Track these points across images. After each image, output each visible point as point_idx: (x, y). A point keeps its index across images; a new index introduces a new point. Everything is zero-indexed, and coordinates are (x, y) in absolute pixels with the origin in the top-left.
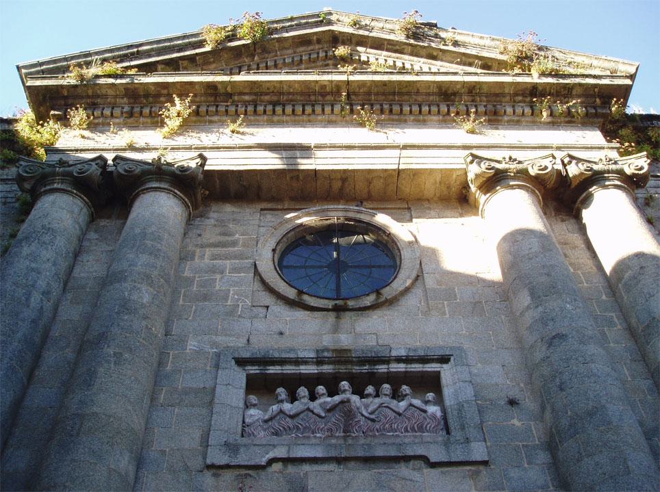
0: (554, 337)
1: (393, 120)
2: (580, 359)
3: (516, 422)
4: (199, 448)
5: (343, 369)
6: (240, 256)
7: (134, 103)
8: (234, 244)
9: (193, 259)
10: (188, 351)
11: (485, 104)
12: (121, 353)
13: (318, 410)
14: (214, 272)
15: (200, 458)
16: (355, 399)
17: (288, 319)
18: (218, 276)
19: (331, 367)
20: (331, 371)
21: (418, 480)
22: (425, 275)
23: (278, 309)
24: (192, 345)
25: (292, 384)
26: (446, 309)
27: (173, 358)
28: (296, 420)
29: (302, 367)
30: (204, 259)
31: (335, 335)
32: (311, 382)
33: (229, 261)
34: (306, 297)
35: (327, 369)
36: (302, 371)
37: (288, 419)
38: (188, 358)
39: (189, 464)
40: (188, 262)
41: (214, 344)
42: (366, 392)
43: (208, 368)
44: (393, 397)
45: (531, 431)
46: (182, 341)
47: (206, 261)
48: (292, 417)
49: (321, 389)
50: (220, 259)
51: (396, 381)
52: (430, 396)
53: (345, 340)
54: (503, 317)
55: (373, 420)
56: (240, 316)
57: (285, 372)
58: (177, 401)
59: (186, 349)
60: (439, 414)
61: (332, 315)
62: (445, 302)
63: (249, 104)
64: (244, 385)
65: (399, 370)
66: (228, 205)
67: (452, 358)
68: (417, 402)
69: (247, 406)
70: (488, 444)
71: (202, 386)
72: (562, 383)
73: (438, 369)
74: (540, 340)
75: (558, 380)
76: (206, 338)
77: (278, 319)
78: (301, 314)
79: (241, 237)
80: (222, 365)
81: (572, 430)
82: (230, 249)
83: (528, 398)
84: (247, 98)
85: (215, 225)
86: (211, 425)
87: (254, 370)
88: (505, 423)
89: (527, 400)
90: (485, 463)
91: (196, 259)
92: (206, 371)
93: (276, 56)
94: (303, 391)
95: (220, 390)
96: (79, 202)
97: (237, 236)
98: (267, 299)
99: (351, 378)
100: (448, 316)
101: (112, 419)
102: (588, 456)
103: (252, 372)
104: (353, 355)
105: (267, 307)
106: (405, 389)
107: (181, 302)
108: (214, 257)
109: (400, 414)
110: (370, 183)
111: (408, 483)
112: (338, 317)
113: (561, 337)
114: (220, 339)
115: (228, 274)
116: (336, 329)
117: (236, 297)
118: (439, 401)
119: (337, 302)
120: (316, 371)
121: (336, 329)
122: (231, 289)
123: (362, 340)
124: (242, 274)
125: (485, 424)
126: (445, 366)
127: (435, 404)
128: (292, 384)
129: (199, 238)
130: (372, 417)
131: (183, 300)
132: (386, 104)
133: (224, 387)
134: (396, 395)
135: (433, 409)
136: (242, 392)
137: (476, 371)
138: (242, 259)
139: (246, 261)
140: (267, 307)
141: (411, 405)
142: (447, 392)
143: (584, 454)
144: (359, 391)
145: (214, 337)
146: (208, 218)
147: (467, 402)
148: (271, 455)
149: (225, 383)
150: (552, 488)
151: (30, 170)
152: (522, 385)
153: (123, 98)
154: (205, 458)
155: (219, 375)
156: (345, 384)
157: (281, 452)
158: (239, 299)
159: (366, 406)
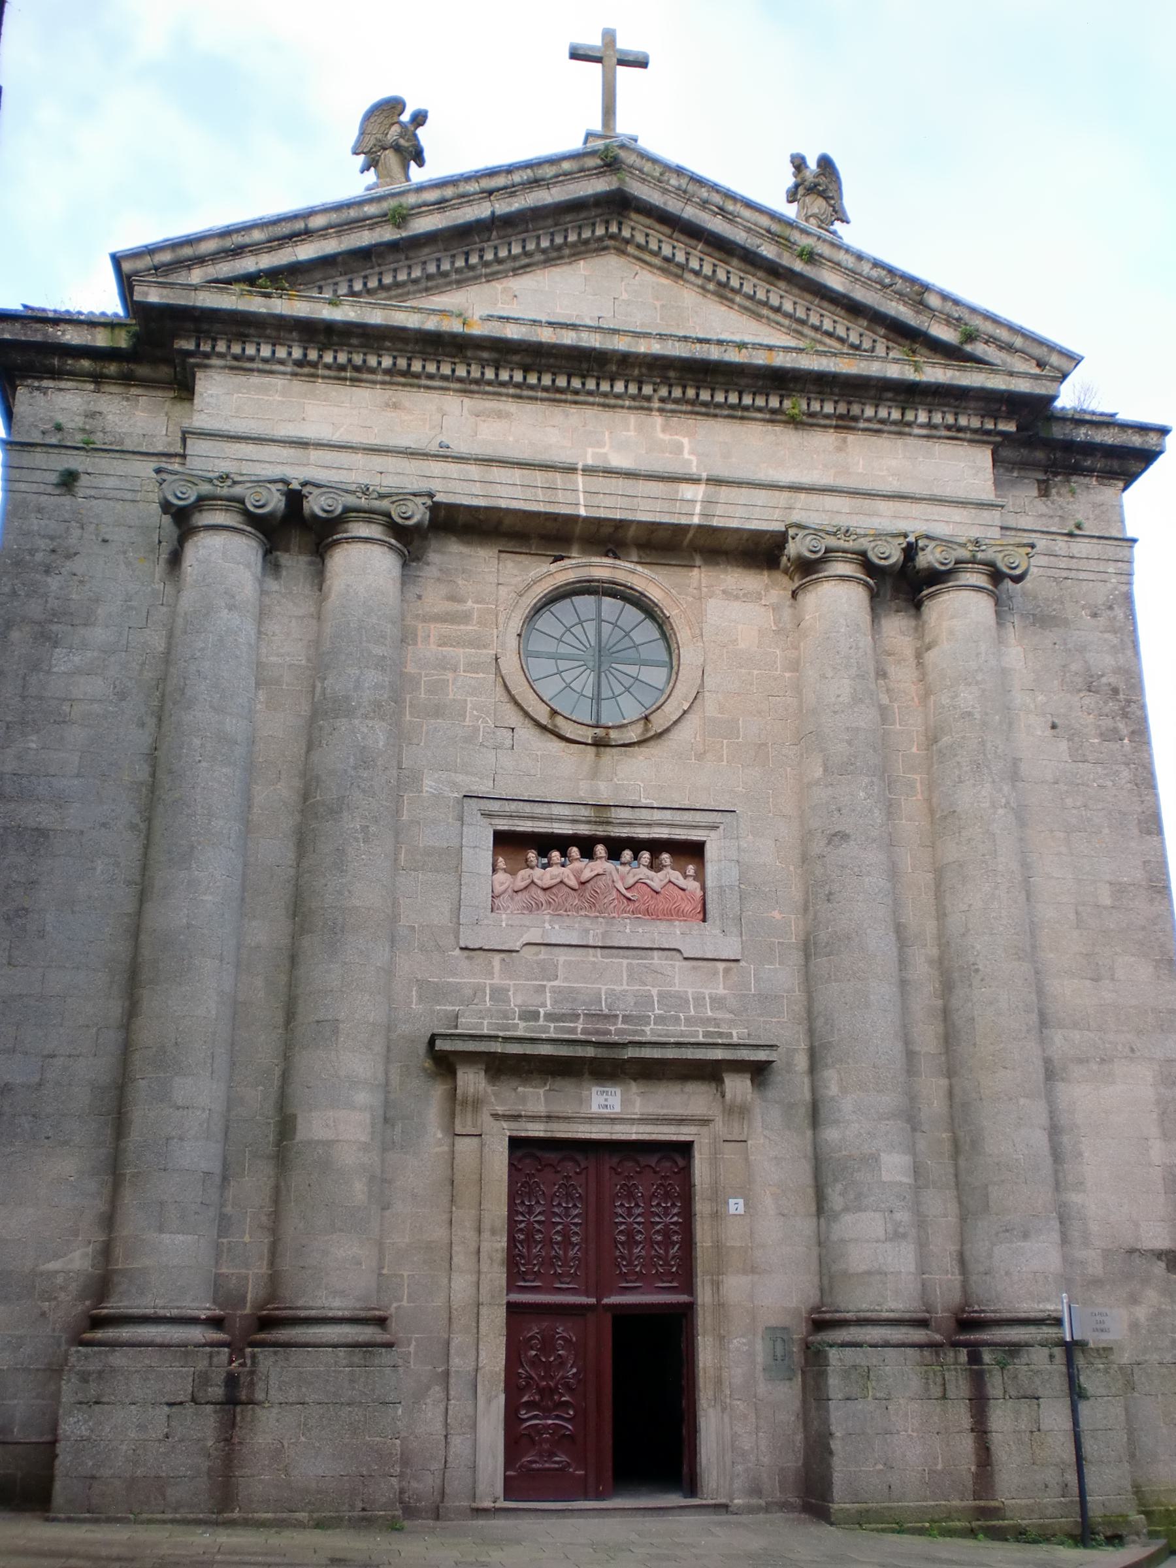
0: (835, 835)
1: (697, 413)
2: (856, 869)
3: (776, 914)
4: (450, 924)
5: (600, 831)
6: (476, 643)
7: (310, 341)
8: (465, 618)
9: (415, 644)
10: (424, 794)
11: (836, 398)
12: (368, 827)
13: (573, 882)
14: (445, 669)
15: (452, 937)
16: (610, 866)
17: (539, 753)
18: (450, 676)
19: (587, 827)
20: (587, 833)
21: (670, 974)
22: (707, 694)
23: (527, 733)
24: (429, 784)
26: (725, 752)
27: (409, 804)
28: (548, 892)
29: (555, 825)
30: (429, 643)
31: (593, 782)
32: (561, 843)
33: (462, 650)
34: (560, 721)
35: (584, 830)
36: (556, 831)
37: (539, 891)
38: (426, 804)
39: (440, 943)
40: (409, 647)
41: (454, 785)
42: (623, 860)
43: (450, 820)
44: (651, 866)
45: (790, 926)
46: (416, 779)
47: (433, 647)
48: (545, 890)
49: (574, 851)
50: (451, 646)
51: (656, 847)
52: (691, 869)
53: (604, 793)
54: (789, 769)
55: (629, 899)
56: (482, 745)
57: (536, 830)
58: (420, 864)
59: (422, 792)
60: (699, 893)
61: (591, 750)
62: (725, 741)
63: (488, 365)
64: (491, 844)
65: (662, 836)
66: (454, 539)
67: (722, 827)
68: (676, 876)
69: (494, 870)
70: (744, 938)
71: (445, 845)
72: (830, 893)
73: (704, 839)
74: (820, 831)
75: (827, 887)
76: (444, 775)
77: (528, 752)
78: (557, 745)
79: (476, 606)
80: (467, 819)
81: (828, 949)
82: (462, 627)
83: (796, 885)
84: (485, 355)
85: (438, 579)
86: (460, 899)
87: (504, 825)
88: (765, 915)
89: (793, 889)
90: (737, 961)
91: (419, 642)
92: (448, 824)
93: (527, 231)
95: (466, 853)
96: (254, 544)
97: (470, 603)
98: (513, 717)
99: (608, 841)
100: (725, 763)
101: (371, 912)
102: (836, 981)
103: (499, 828)
104: (613, 816)
105: (513, 729)
106: (666, 857)
107: (408, 718)
108: (444, 641)
109: (657, 893)
110: (652, 532)
111: (659, 976)
112: (598, 755)
113: (844, 837)
114: (460, 778)
115: (462, 673)
116: (594, 774)
117: (475, 712)
118: (700, 876)
119: (597, 730)
120: (571, 832)
121: (594, 774)
122: (469, 699)
123: (624, 792)
124: (481, 675)
125: (744, 914)
127: (696, 878)
129: (419, 603)
130: (629, 895)
131: (411, 713)
132: (691, 386)
133: (471, 851)
134: (654, 866)
135: (693, 885)
136: (490, 854)
137: (745, 845)
138: (478, 648)
139: (485, 651)
140: (513, 729)
141: (670, 881)
142: (710, 868)
143: (833, 978)
145: (453, 774)
146: (428, 564)
147: (731, 887)
148: (526, 938)
149: (472, 844)
150: (797, 993)
151: (183, 493)
152: (792, 868)
153: (291, 331)
154: (457, 937)
155: (465, 833)
156: (600, 850)
157: (534, 935)
158: (478, 719)
159: (623, 878)
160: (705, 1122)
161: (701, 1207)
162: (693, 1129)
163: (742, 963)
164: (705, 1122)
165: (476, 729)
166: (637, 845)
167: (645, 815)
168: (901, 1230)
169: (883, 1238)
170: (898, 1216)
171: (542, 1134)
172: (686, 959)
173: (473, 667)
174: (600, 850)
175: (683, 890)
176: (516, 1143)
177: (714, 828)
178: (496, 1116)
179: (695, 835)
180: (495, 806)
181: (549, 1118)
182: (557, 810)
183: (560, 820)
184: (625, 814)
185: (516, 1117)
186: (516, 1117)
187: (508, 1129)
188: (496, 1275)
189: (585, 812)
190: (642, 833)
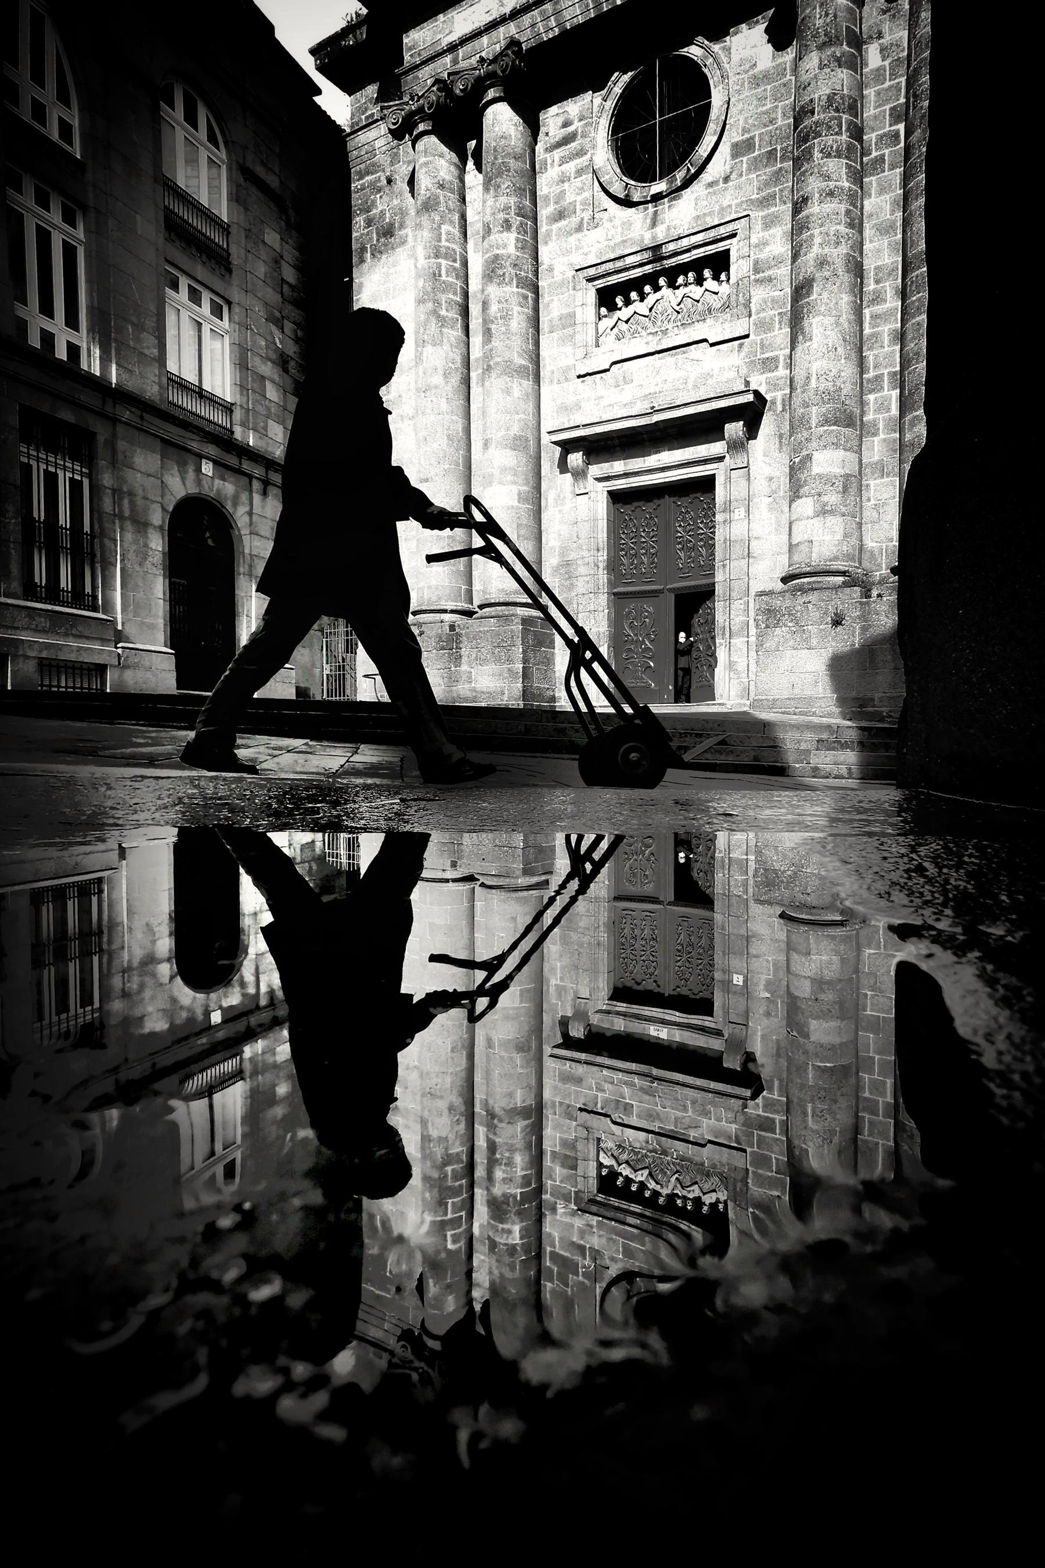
5: (658, 267)
18: (566, 184)
25: (625, 289)
32: (637, 284)
35: (648, 269)
48: (627, 322)
51: (697, 266)
53: (661, 233)
87: (600, 283)
90: (747, 336)
94: (634, 295)
99: (664, 272)
109: (698, 301)
116: (654, 224)
121: (654, 224)
126: (734, 241)
128: (625, 289)
134: (700, 281)
144: (672, 285)
160: (720, 459)
161: (719, 518)
162: (715, 466)
163: (752, 337)
164: (720, 459)
165: (582, 219)
166: (683, 269)
167: (685, 243)
168: (828, 508)
169: (811, 514)
170: (825, 499)
171: (625, 486)
172: (712, 345)
173: (580, 172)
174: (662, 281)
175: (716, 293)
176: (616, 497)
177: (733, 236)
178: (599, 480)
179: (721, 246)
180: (592, 272)
181: (626, 475)
182: (630, 260)
183: (634, 267)
184: (671, 247)
185: (607, 478)
186: (607, 478)
187: (603, 488)
188: (603, 577)
189: (646, 256)
190: (685, 258)
